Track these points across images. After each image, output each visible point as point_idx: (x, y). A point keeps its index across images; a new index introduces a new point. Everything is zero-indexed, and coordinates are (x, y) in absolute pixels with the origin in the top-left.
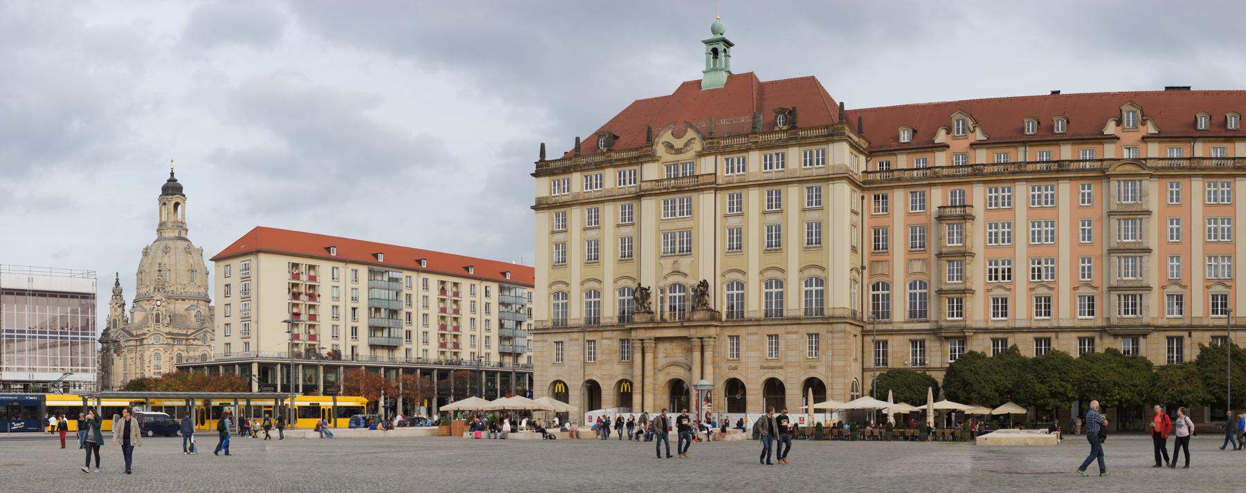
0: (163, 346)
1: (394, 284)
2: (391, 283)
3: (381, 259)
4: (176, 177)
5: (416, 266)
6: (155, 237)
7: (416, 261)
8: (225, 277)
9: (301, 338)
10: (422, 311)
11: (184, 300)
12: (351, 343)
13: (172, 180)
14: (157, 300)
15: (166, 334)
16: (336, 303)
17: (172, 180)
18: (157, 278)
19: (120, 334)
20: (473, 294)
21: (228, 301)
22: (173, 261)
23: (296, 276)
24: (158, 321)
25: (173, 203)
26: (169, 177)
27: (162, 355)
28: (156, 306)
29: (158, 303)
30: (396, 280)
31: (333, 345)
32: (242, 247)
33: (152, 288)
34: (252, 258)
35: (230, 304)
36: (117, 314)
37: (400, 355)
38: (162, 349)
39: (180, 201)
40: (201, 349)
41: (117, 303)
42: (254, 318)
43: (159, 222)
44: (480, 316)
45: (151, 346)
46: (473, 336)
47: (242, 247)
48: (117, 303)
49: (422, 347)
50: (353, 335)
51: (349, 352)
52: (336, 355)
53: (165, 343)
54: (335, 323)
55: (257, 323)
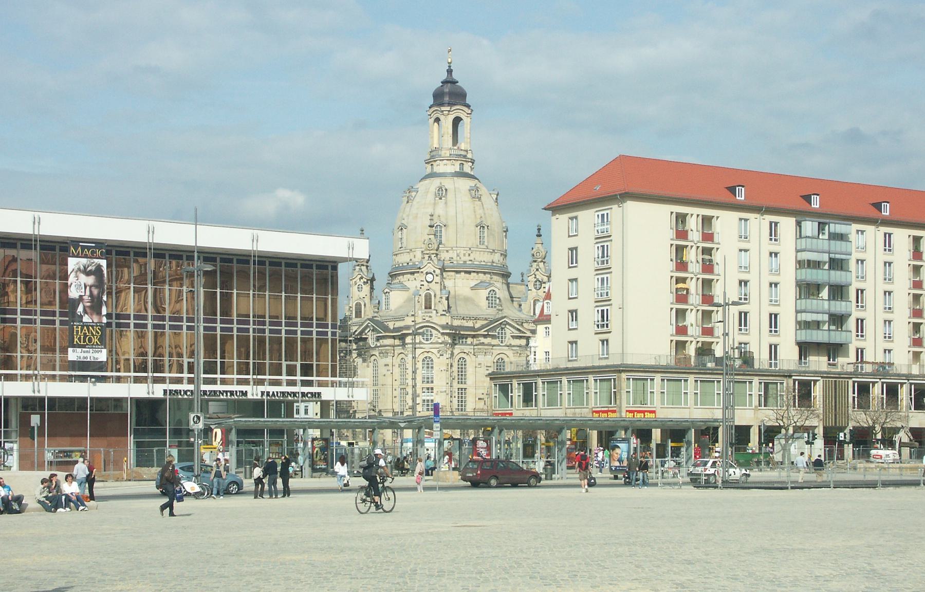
1: (838, 243)
2: (832, 242)
4: (455, 76)
5: (873, 213)
8: (569, 236)
9: (690, 332)
11: (469, 273)
12: (767, 339)
13: (450, 82)
14: (427, 273)
15: (443, 327)
16: (744, 277)
17: (450, 82)
18: (427, 237)
19: (367, 326)
21: (573, 273)
22: (452, 211)
23: (682, 234)
24: (428, 306)
25: (451, 118)
26: (444, 76)
27: (435, 360)
28: (425, 283)
29: (430, 278)
30: (841, 237)
33: (419, 255)
35: (576, 280)
36: (362, 294)
38: (435, 351)
39: (462, 116)
40: (496, 351)
41: (362, 278)
48: (362, 278)
49: (882, 345)
50: (771, 327)
51: (765, 355)
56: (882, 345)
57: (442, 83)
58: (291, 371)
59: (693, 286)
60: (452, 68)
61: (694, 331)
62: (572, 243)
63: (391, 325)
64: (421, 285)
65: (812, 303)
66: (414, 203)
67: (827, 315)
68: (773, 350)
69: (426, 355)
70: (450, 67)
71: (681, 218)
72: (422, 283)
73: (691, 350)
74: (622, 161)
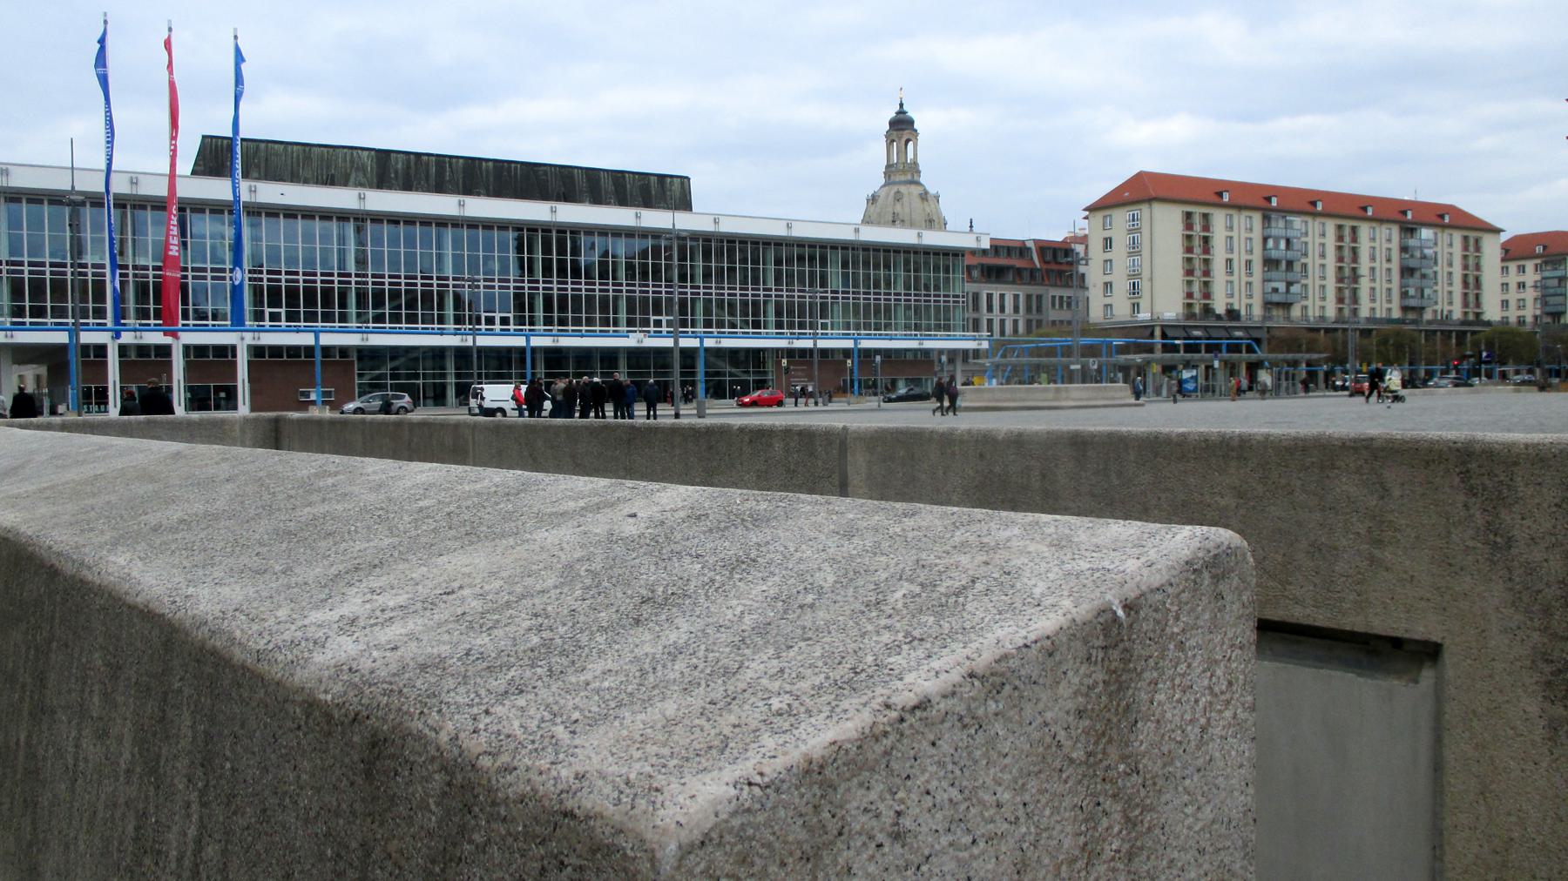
3: (1274, 202)
7: (1309, 204)
10: (1377, 265)
20: (1373, 239)
21: (1108, 256)
23: (1189, 226)
31: (1227, 304)
32: (1127, 194)
34: (1145, 208)
37: (1296, 312)
42: (1146, 274)
44: (1381, 265)
46: (1373, 289)
47: (1127, 194)
49: (1319, 303)
55: (1151, 279)
56: (1319, 303)
58: (490, 321)
59: (1197, 264)
61: (1197, 294)
62: (1107, 234)
65: (1274, 274)
71: (1189, 215)
73: (1197, 310)
74: (1140, 177)
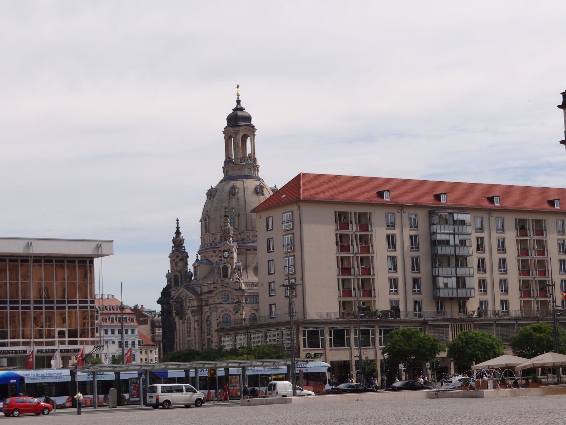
0: (233, 305)
1: (460, 227)
2: (456, 227)
4: (242, 105)
6: (221, 176)
13: (239, 108)
14: (224, 251)
17: (239, 108)
25: (240, 136)
26: (235, 105)
28: (223, 258)
31: (391, 301)
33: (218, 238)
38: (232, 309)
39: (248, 134)
43: (224, 159)
45: (218, 306)
52: (395, 309)
53: (235, 301)
54: (394, 275)
57: (233, 110)
60: (240, 99)
63: (199, 290)
64: (220, 260)
66: (215, 199)
67: (454, 279)
68: (417, 304)
69: (225, 312)
70: (238, 98)
72: (221, 259)
